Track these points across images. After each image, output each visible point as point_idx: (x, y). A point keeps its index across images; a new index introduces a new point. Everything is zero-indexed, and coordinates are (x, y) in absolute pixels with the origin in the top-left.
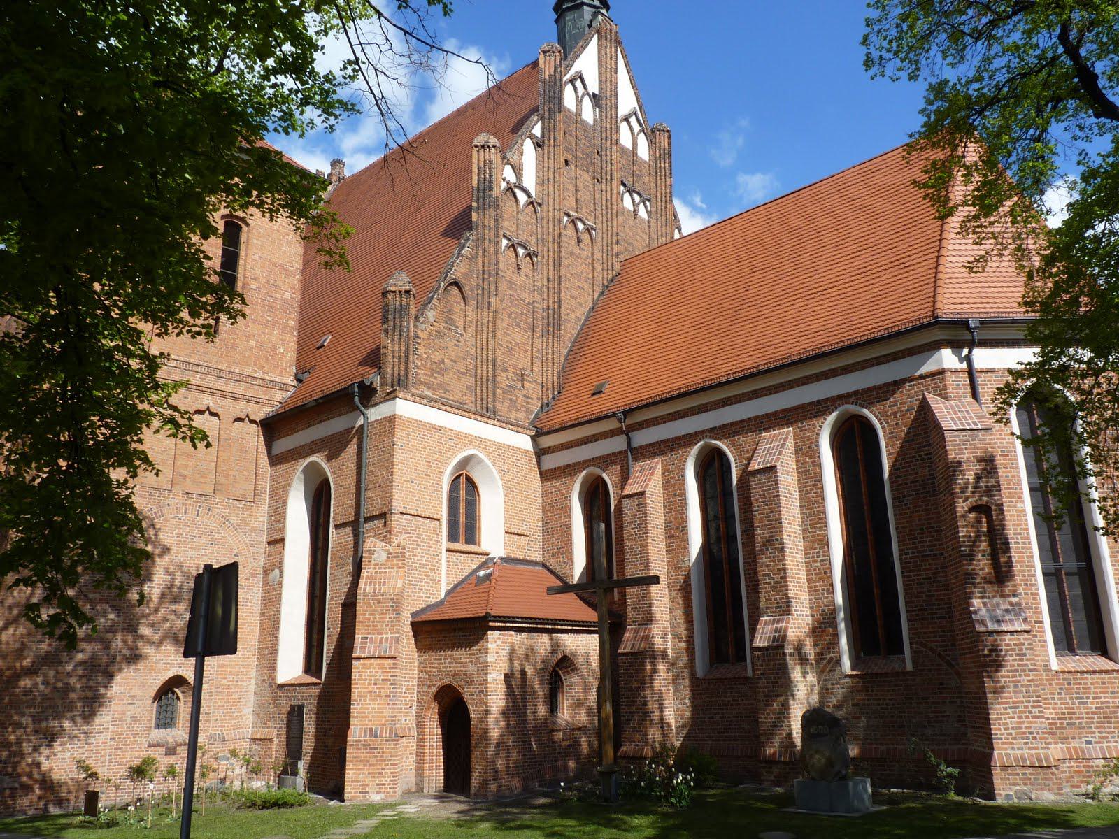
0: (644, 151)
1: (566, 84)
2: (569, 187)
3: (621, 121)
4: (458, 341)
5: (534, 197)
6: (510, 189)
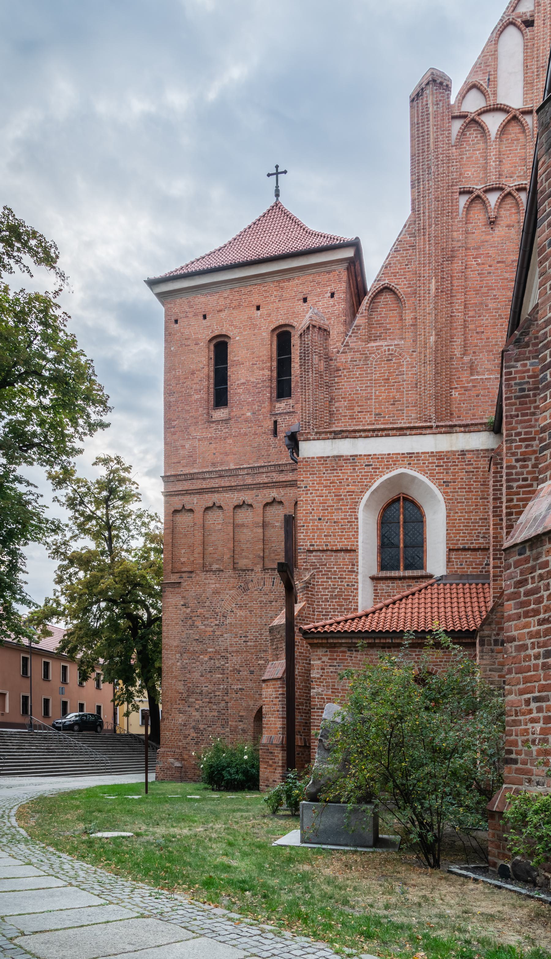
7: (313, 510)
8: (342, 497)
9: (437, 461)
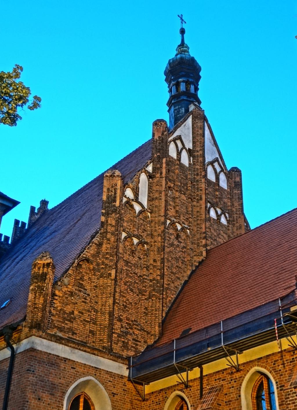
0: (223, 183)
1: (170, 142)
2: (171, 203)
3: (208, 165)
4: (85, 299)
5: (146, 208)
6: (128, 202)
7: (36, 390)
8: (55, 386)
9: (109, 378)
